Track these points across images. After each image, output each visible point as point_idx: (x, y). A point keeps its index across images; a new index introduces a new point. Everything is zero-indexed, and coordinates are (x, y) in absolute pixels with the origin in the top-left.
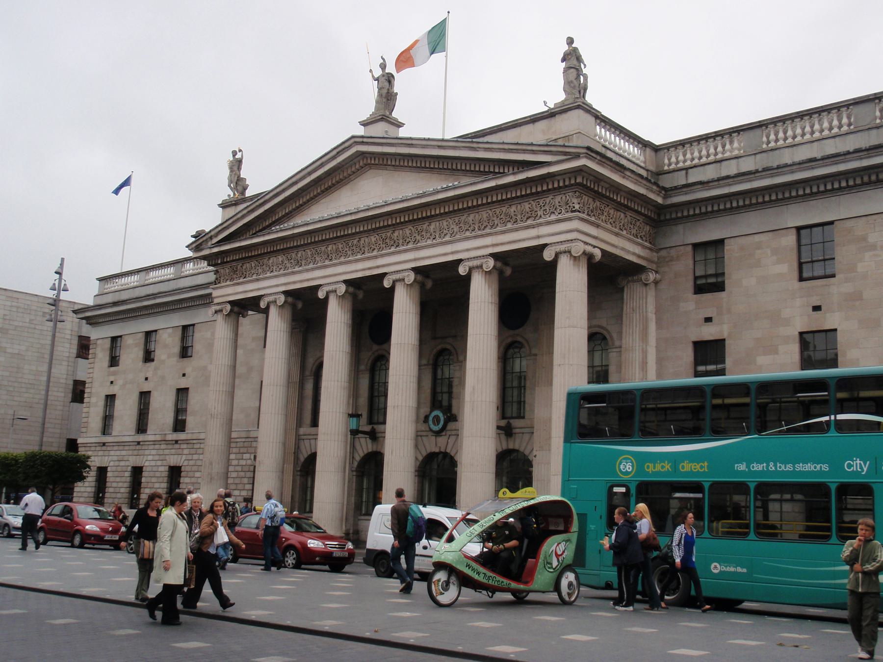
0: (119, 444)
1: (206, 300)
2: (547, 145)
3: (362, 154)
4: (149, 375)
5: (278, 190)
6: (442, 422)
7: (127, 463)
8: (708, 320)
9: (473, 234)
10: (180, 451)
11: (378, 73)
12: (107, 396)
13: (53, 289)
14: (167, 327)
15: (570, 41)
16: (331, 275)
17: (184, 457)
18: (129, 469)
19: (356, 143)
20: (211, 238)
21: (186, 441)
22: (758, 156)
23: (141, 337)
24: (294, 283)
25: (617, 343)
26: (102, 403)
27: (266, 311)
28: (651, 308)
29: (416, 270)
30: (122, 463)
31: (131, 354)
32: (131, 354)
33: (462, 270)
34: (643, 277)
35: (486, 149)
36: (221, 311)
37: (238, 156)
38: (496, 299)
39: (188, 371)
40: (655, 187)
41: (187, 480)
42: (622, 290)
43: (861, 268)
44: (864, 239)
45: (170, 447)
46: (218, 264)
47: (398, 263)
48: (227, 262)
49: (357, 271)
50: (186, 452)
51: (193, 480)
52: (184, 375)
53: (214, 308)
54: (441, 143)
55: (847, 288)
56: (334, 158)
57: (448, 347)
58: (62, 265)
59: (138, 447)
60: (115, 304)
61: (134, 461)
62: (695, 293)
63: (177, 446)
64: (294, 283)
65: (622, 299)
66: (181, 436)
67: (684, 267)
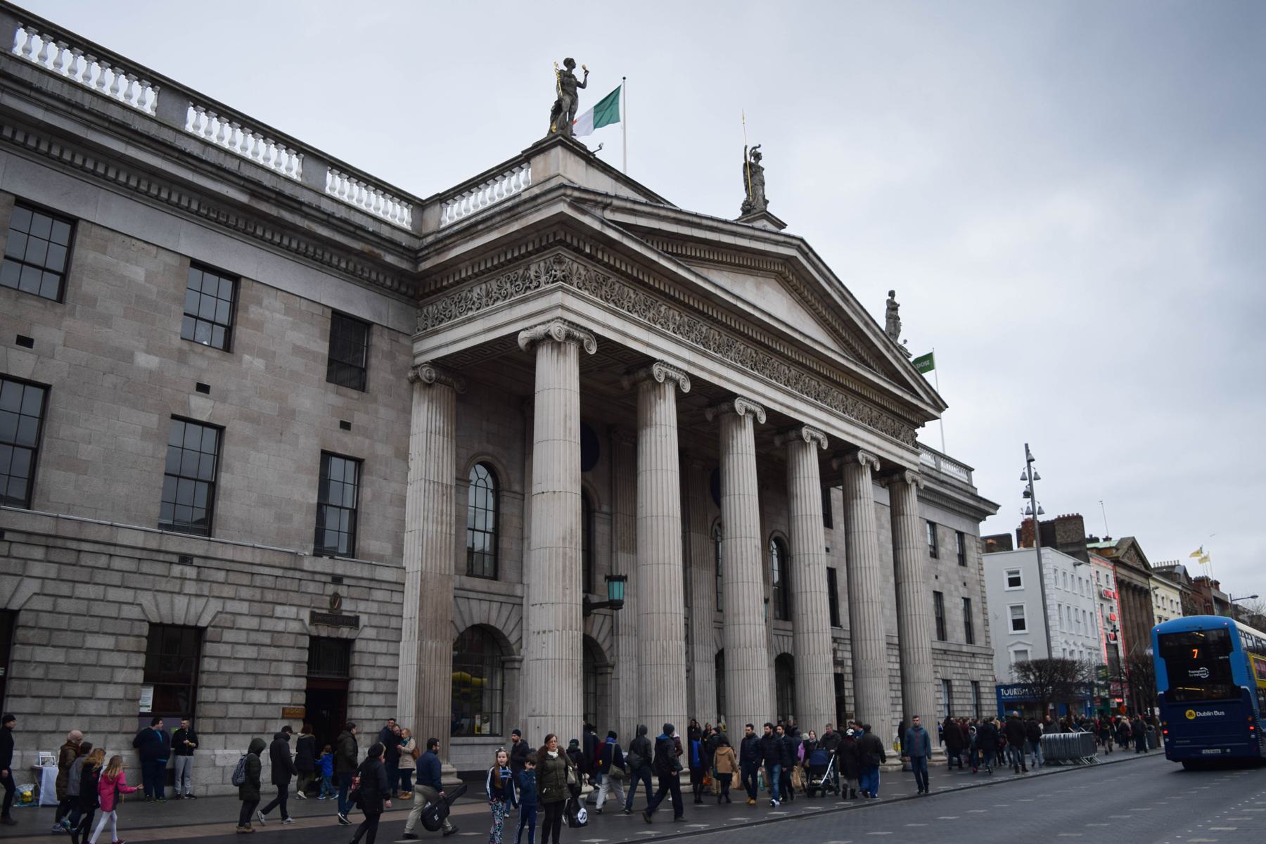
5: (720, 225)
10: (14, 566)
15: (892, 294)
17: (31, 586)
19: (799, 249)
20: (605, 207)
21: (50, 542)
24: (703, 369)
39: (35, 334)
48: (600, 261)
49: (775, 401)
50: (37, 569)
51: (78, 656)
52: (25, 342)
64: (703, 369)
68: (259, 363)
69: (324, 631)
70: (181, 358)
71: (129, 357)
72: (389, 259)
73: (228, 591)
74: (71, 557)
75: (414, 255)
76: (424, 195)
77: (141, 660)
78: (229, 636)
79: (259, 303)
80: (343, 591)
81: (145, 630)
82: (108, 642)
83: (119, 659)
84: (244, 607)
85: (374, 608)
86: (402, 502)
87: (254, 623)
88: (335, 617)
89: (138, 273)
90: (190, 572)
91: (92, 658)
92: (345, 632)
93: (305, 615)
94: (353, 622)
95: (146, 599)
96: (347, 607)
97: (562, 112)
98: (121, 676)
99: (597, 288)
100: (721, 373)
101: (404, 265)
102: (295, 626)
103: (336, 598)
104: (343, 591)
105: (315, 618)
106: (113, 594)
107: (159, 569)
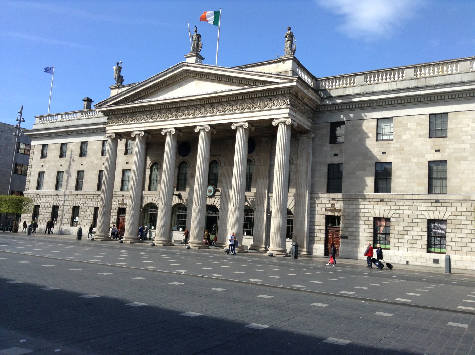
0: (46, 195)
1: (102, 131)
2: (279, 75)
3: (187, 71)
4: (63, 163)
6: (213, 192)
7: (51, 204)
8: (336, 155)
9: (239, 111)
12: (40, 172)
13: (18, 120)
14: (73, 143)
16: (168, 124)
17: (81, 202)
18: (52, 206)
20: (107, 103)
21: (83, 195)
22: (362, 87)
23: (59, 146)
25: (295, 162)
26: (37, 175)
27: (134, 139)
28: (311, 148)
29: (210, 125)
30: (48, 204)
31: (53, 153)
32: (53, 153)
33: (233, 128)
34: (309, 135)
35: (249, 74)
36: (110, 137)
37: (120, 65)
38: (247, 140)
40: (318, 97)
41: (82, 213)
42: (298, 140)
43: (404, 137)
44: (406, 125)
45: (74, 197)
46: (109, 115)
47: (202, 121)
48: (114, 114)
52: (82, 165)
53: (106, 135)
55: (397, 145)
56: (172, 71)
57: (216, 160)
58: (22, 109)
59: (56, 197)
60: (46, 129)
61: (54, 203)
62: (330, 143)
65: (298, 144)
66: (79, 192)
67: (327, 131)
70: (101, 159)
71: (93, 162)
80: (124, 198)
81: (94, 208)
89: (95, 147)
93: (117, 203)
94: (126, 204)
103: (123, 200)
104: (124, 198)
105: (119, 204)
107: (96, 197)
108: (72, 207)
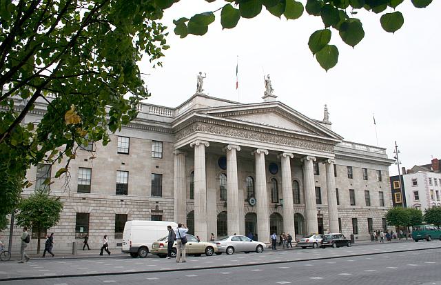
11: (266, 79)
15: (326, 106)
17: (91, 208)
21: (93, 199)
37: (203, 75)
47: (289, 150)
54: (308, 119)
63: (84, 201)
68: (136, 156)
69: (154, 214)
70: (118, 158)
72: (165, 126)
73: (132, 206)
74: (99, 202)
75: (171, 124)
76: (174, 107)
77: (114, 222)
78: (132, 216)
79: (134, 142)
80: (159, 204)
82: (108, 218)
83: (110, 222)
84: (136, 210)
85: (167, 208)
86: (173, 183)
87: (138, 213)
88: (157, 211)
90: (124, 203)
91: (104, 221)
92: (160, 214)
93: (150, 210)
94: (162, 211)
95: (115, 209)
96: (160, 208)
97: (199, 87)
98: (110, 225)
99: (210, 130)
100: (250, 143)
101: (170, 127)
102: (148, 213)
103: (157, 206)
104: (159, 204)
106: (108, 209)
107: (116, 203)
108: (76, 214)
